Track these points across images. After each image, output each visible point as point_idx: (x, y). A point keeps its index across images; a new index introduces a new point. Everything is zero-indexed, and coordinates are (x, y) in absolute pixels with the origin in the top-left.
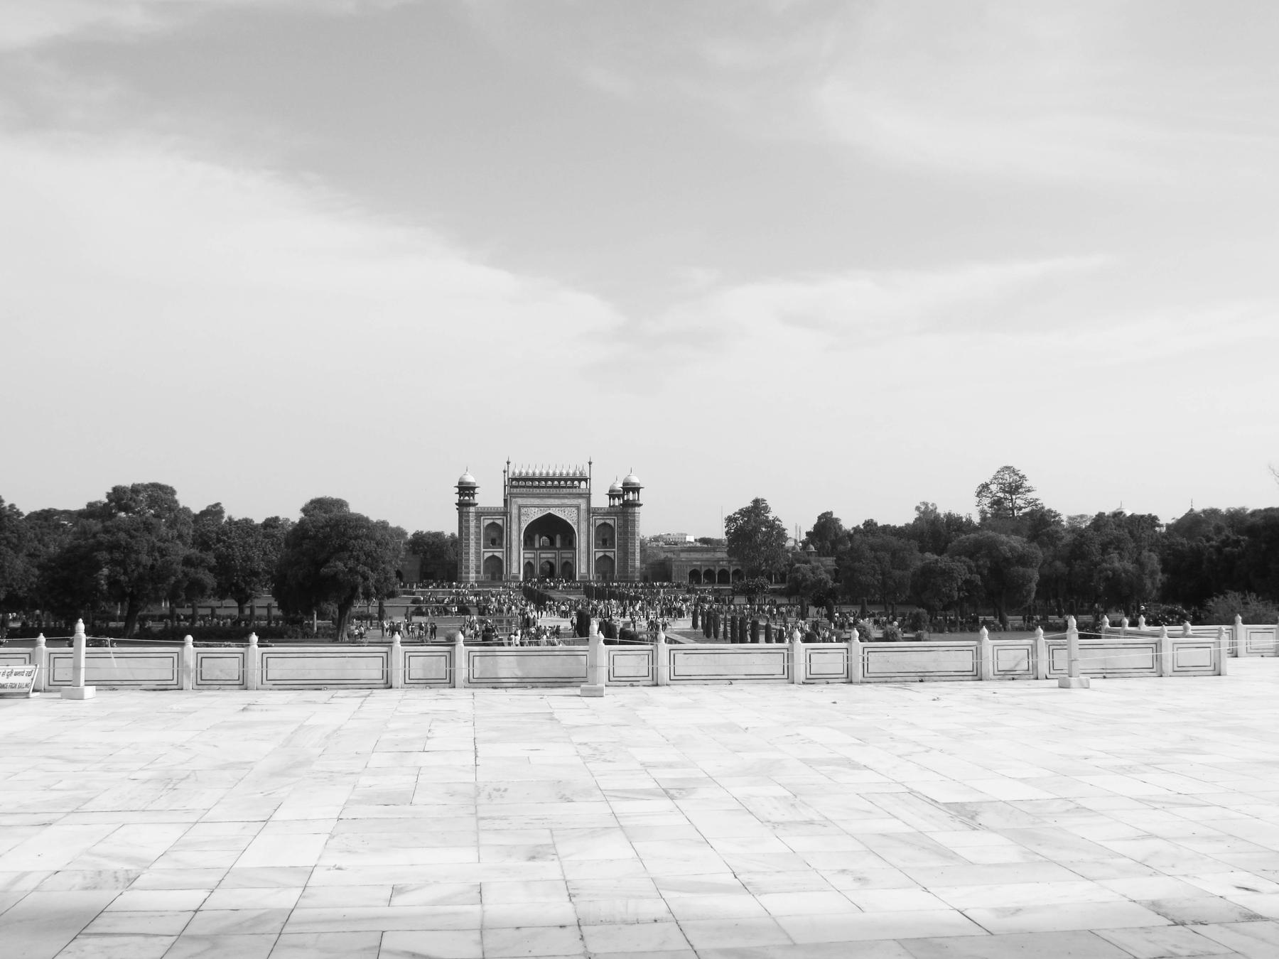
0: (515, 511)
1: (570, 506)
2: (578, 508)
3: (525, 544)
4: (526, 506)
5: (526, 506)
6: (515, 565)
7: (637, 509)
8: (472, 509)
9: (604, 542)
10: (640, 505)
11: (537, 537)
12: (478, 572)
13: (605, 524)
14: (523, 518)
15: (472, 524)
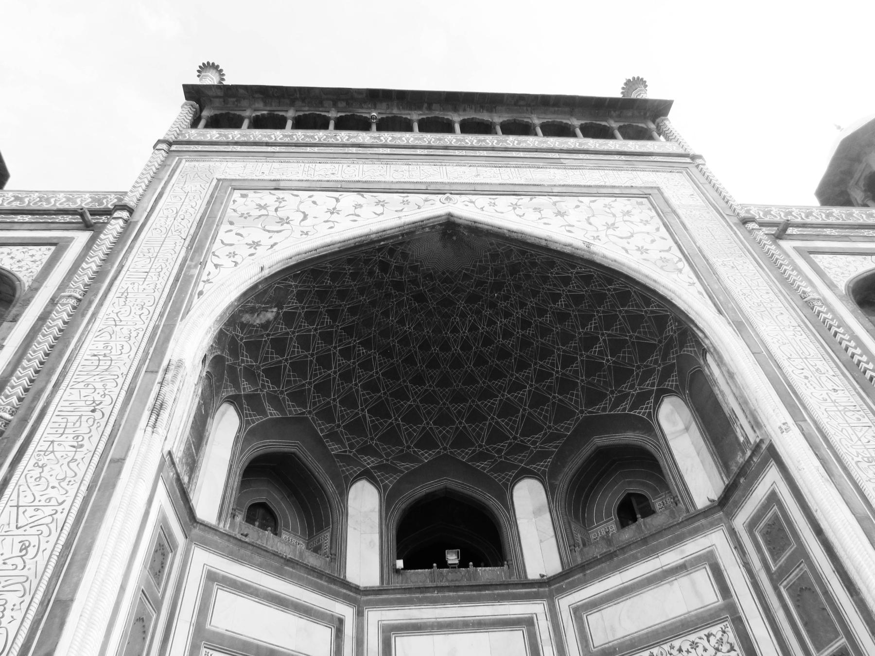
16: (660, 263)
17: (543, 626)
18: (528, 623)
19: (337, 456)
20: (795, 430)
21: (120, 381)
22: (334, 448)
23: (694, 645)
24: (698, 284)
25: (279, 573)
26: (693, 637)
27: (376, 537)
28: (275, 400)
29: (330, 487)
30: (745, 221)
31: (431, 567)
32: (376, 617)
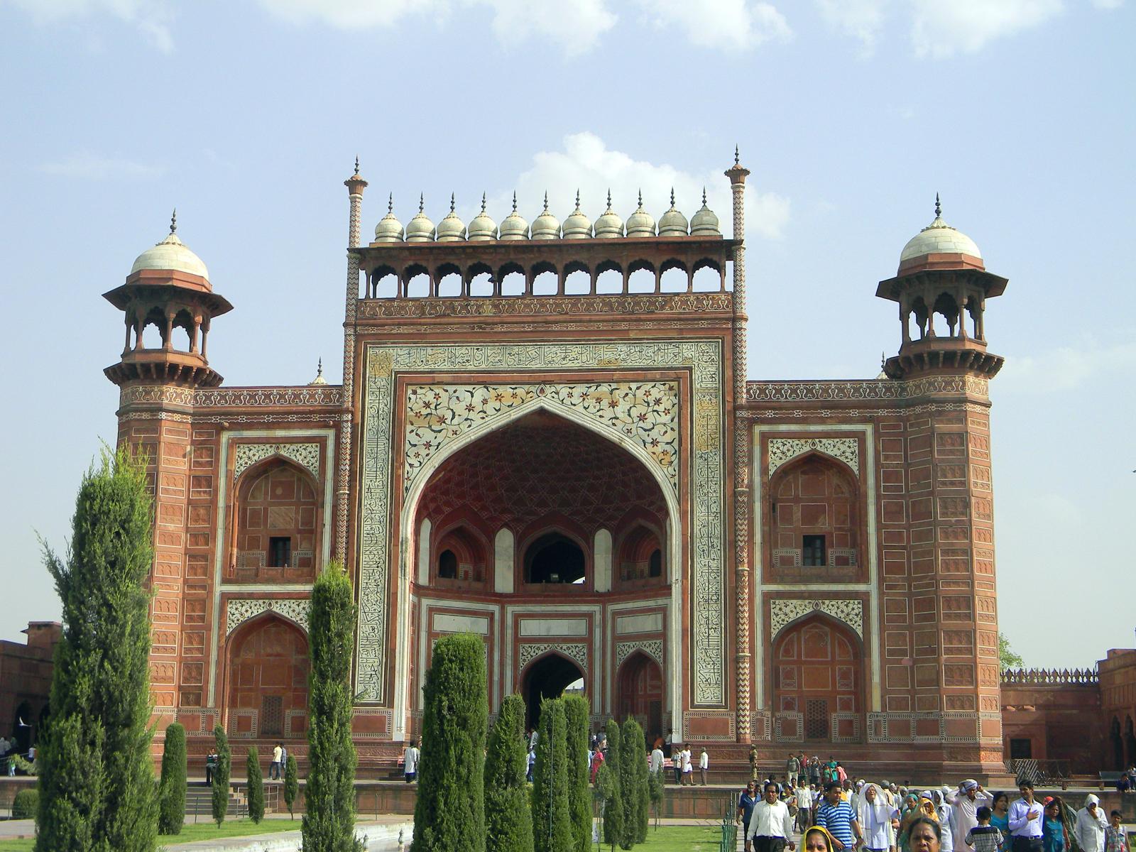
0: (376, 405)
1: (641, 375)
2: (679, 379)
3: (445, 564)
4: (430, 379)
5: (430, 379)
6: (367, 661)
7: (970, 378)
8: (177, 396)
9: (814, 546)
10: (989, 365)
11: (505, 541)
12: (191, 695)
13: (813, 463)
14: (411, 438)
15: (176, 464)
16: (661, 456)
17: (598, 618)
18: (589, 616)
19: (487, 519)
20: (680, 583)
21: (384, 549)
22: (485, 515)
23: (650, 645)
24: (677, 477)
25: (460, 598)
26: (650, 642)
27: (512, 563)
28: (448, 504)
29: (484, 539)
30: (736, 408)
31: (541, 582)
32: (510, 609)
